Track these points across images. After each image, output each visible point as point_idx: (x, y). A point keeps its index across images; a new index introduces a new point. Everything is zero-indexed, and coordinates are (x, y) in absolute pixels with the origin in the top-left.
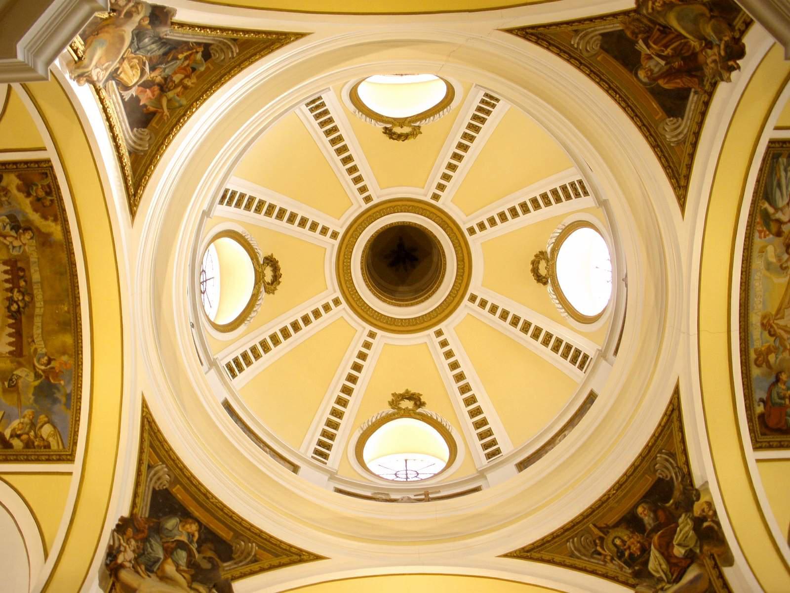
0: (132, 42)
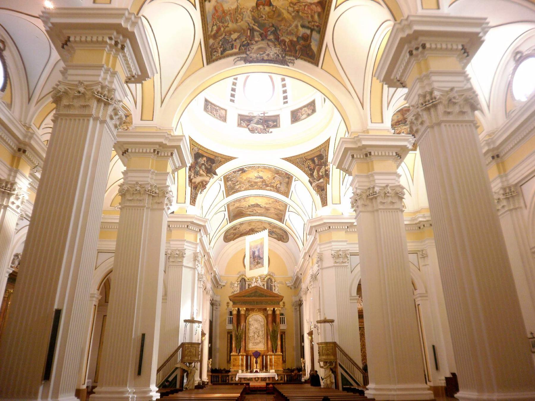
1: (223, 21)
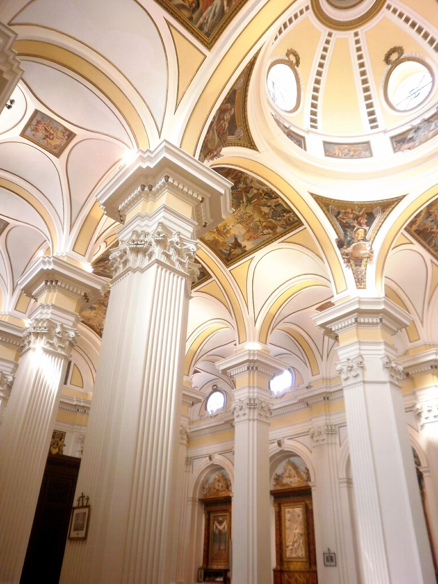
0: (353, 243)
1: (257, 227)
